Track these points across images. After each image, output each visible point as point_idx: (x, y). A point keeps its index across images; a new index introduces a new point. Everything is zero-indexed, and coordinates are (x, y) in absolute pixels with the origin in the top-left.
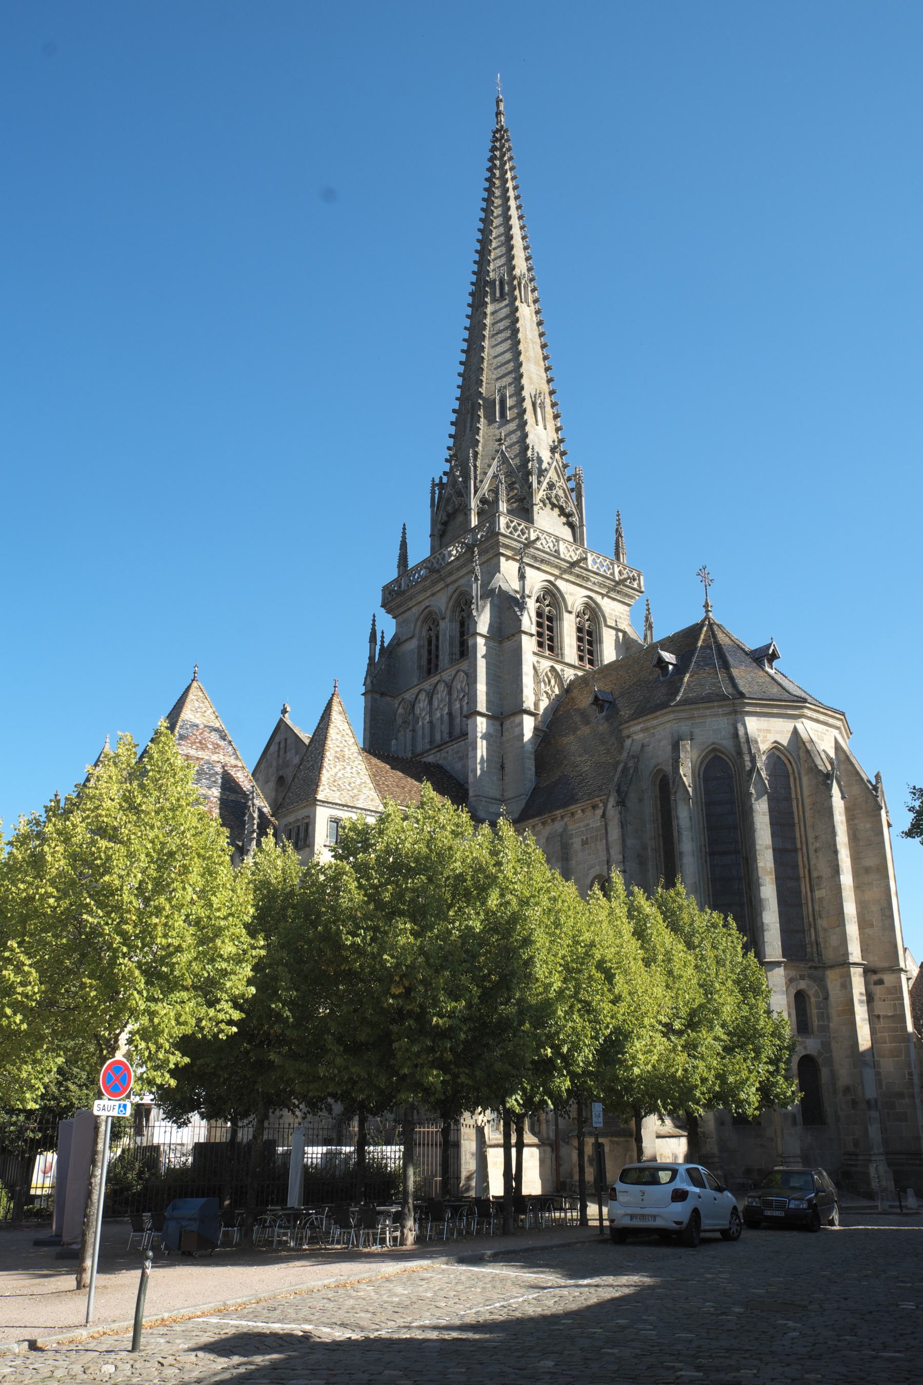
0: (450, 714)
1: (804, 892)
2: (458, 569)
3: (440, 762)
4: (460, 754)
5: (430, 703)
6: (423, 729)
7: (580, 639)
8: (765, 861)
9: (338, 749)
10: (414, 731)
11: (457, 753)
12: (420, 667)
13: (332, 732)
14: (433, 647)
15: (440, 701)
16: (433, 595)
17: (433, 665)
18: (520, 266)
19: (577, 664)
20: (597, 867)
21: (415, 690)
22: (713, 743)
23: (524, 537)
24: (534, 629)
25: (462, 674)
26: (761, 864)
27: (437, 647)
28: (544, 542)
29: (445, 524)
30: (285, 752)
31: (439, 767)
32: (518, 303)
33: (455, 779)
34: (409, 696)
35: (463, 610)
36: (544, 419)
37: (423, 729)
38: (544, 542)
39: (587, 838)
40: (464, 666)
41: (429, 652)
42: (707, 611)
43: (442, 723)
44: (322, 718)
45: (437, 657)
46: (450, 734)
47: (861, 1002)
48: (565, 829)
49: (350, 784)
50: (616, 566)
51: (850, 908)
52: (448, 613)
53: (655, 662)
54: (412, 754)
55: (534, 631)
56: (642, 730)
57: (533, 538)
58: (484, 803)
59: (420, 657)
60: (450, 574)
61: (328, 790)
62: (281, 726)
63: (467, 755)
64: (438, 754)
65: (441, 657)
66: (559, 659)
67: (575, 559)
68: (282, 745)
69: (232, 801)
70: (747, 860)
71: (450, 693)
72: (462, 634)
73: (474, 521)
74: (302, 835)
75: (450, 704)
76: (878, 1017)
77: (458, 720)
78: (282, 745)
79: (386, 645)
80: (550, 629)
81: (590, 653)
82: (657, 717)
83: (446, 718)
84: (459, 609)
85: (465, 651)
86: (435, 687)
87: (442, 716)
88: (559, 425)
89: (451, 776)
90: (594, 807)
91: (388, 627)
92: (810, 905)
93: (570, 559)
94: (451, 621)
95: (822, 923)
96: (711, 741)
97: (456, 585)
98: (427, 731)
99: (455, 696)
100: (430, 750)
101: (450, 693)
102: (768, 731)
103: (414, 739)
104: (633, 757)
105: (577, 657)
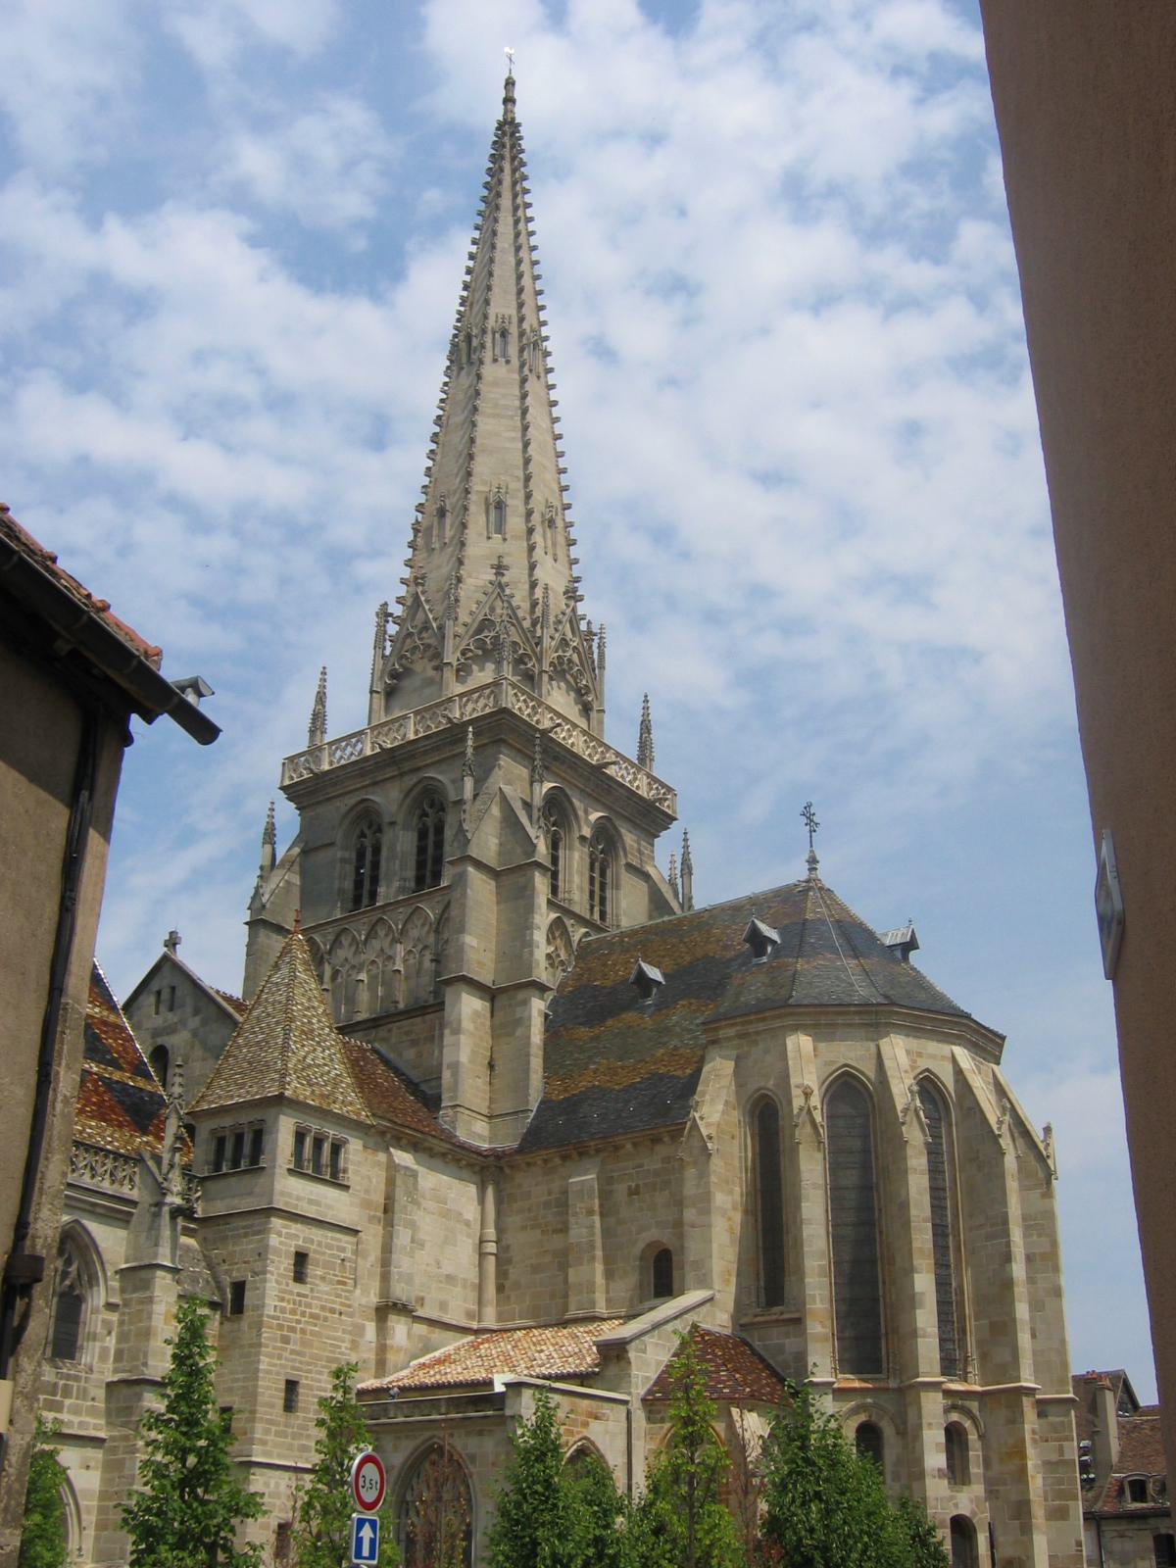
2: (426, 752)
4: (413, 1036)
8: (922, 1238)
11: (407, 1033)
16: (375, 784)
26: (916, 1244)
35: (427, 815)
39: (637, 1186)
42: (812, 869)
49: (322, 1076)
60: (412, 757)
66: (566, 906)
68: (166, 995)
69: (117, 1082)
72: (421, 850)
74: (247, 1149)
82: (764, 1019)
84: (418, 812)
96: (843, 1061)
97: (413, 779)
102: (920, 1055)
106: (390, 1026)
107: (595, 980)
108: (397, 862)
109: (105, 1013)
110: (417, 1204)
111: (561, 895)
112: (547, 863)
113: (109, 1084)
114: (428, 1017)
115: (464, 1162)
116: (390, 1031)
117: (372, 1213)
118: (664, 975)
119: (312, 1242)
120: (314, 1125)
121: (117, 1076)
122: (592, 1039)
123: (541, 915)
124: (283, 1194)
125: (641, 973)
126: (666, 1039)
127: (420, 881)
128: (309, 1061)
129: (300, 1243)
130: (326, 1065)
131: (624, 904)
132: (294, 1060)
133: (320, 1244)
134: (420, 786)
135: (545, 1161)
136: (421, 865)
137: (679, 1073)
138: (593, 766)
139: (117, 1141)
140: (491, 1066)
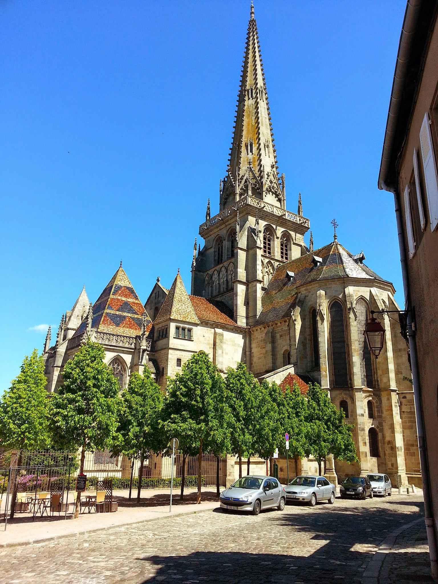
0: (227, 280)
1: (372, 359)
5: (219, 275)
6: (216, 287)
7: (282, 249)
9: (180, 297)
10: (212, 287)
11: (230, 297)
12: (215, 260)
13: (177, 290)
14: (220, 252)
15: (223, 275)
16: (220, 230)
18: (260, 83)
19: (280, 260)
20: (286, 346)
21: (213, 269)
23: (258, 206)
24: (262, 246)
25: (232, 264)
27: (222, 251)
28: (267, 207)
29: (226, 199)
30: (158, 297)
31: (222, 302)
32: (259, 100)
33: (229, 308)
34: (210, 272)
35: (233, 237)
36: (269, 153)
37: (216, 287)
38: (267, 207)
39: (282, 334)
40: (233, 260)
41: (219, 254)
43: (223, 284)
44: (173, 284)
45: (222, 256)
46: (227, 289)
47: (396, 406)
48: (273, 330)
49: (184, 312)
50: (298, 217)
51: (391, 366)
52: (227, 238)
54: (211, 297)
55: (262, 246)
56: (305, 290)
57: (262, 206)
59: (215, 256)
60: (228, 221)
61: (175, 315)
62: (157, 286)
65: (223, 256)
67: (280, 215)
68: (157, 294)
69: (136, 318)
70: (348, 344)
71: (227, 272)
73: (238, 199)
74: (164, 333)
75: (227, 276)
76: (404, 412)
77: (230, 283)
78: (157, 294)
79: (201, 250)
80: (269, 245)
81: (286, 254)
83: (225, 282)
85: (233, 255)
86: (221, 269)
87: (224, 281)
88: (275, 155)
90: (285, 321)
91: (202, 243)
92: (375, 365)
93: (278, 215)
94: (228, 241)
95: (380, 372)
96: (334, 295)
98: (217, 287)
99: (229, 272)
100: (219, 295)
101: (227, 272)
103: (212, 291)
104: (301, 301)
105: (280, 257)
109: (134, 300)
110: (225, 343)
111: (272, 254)
113: (133, 319)
115: (239, 331)
116: (226, 296)
117: (210, 346)
119: (182, 356)
120: (182, 325)
121: (136, 316)
123: (259, 261)
124: (172, 344)
128: (180, 308)
129: (178, 356)
131: (293, 255)
132: (175, 308)
133: (185, 356)
134: (230, 230)
135: (260, 329)
138: (279, 217)
139: (134, 333)
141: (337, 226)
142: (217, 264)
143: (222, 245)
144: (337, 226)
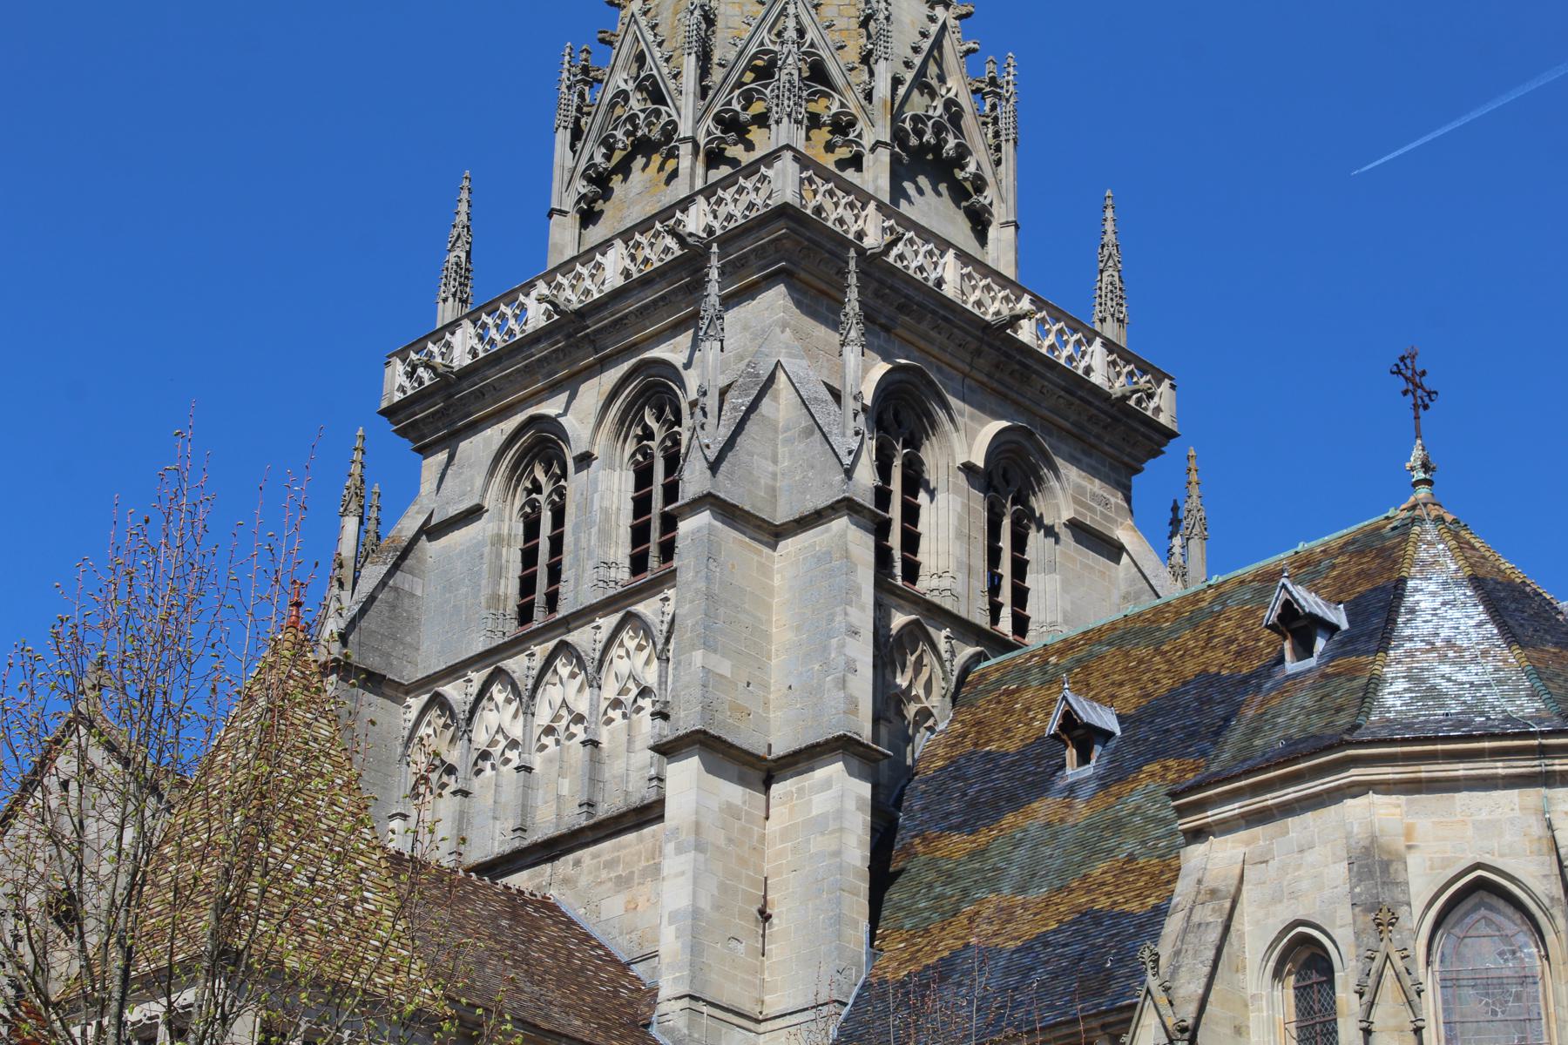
2: (644, 312)
3: (554, 894)
11: (609, 865)
17: (540, 596)
22: (1478, 866)
27: (557, 544)
33: (600, 946)
41: (529, 557)
45: (555, 574)
53: (1272, 614)
58: (705, 1020)
59: (498, 572)
60: (619, 324)
63: (655, 872)
64: (547, 868)
65: (567, 573)
72: (642, 505)
77: (614, 768)
81: (1020, 596)
89: (588, 937)
104: (1213, 893)
106: (579, 853)
107: (986, 744)
108: (594, 530)
112: (868, 501)
114: (647, 831)
116: (577, 863)
118: (1121, 719)
122: (973, 855)
123: (863, 608)
125: (1069, 719)
126: (1112, 843)
127: (638, 564)
130: (340, 889)
136: (640, 535)
137: (1134, 906)
140: (765, 916)
141: (1426, 400)
142: (512, 629)
143: (561, 492)
144: (1426, 400)
